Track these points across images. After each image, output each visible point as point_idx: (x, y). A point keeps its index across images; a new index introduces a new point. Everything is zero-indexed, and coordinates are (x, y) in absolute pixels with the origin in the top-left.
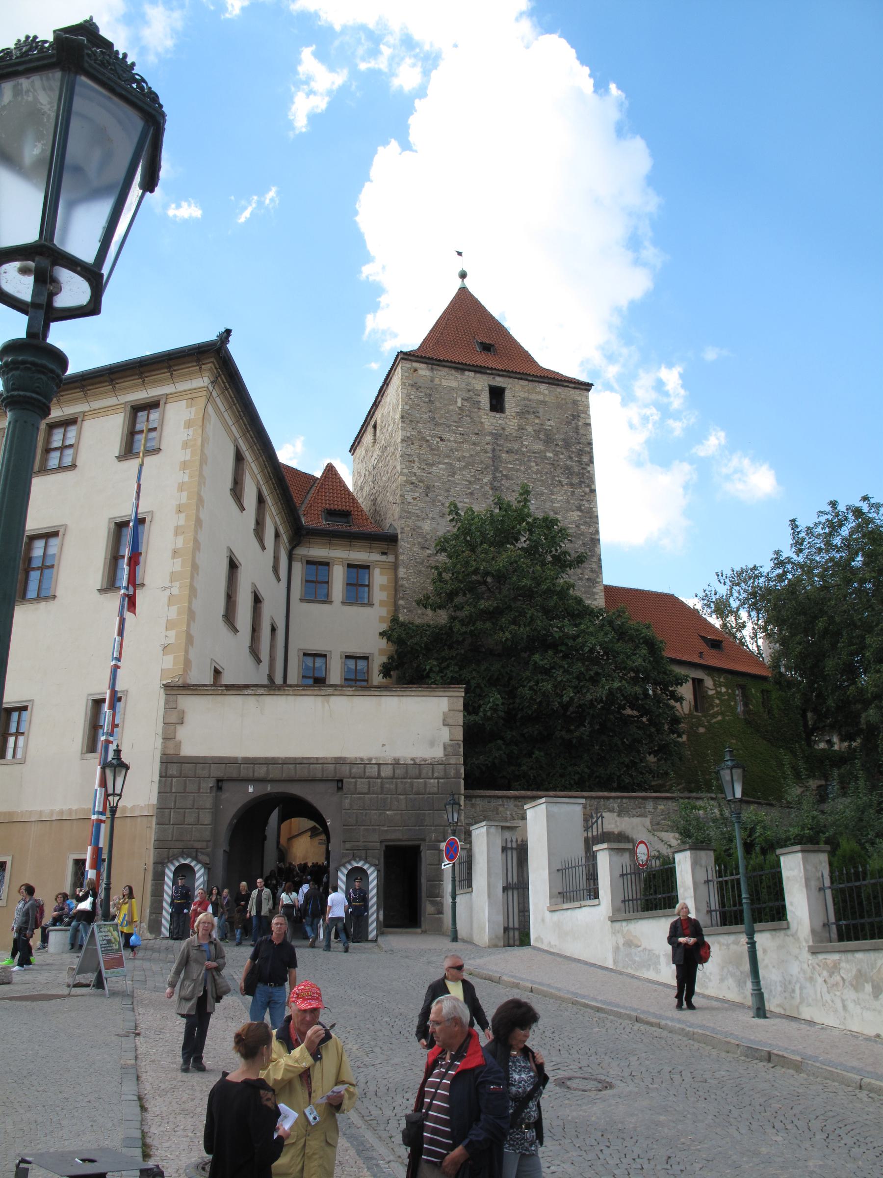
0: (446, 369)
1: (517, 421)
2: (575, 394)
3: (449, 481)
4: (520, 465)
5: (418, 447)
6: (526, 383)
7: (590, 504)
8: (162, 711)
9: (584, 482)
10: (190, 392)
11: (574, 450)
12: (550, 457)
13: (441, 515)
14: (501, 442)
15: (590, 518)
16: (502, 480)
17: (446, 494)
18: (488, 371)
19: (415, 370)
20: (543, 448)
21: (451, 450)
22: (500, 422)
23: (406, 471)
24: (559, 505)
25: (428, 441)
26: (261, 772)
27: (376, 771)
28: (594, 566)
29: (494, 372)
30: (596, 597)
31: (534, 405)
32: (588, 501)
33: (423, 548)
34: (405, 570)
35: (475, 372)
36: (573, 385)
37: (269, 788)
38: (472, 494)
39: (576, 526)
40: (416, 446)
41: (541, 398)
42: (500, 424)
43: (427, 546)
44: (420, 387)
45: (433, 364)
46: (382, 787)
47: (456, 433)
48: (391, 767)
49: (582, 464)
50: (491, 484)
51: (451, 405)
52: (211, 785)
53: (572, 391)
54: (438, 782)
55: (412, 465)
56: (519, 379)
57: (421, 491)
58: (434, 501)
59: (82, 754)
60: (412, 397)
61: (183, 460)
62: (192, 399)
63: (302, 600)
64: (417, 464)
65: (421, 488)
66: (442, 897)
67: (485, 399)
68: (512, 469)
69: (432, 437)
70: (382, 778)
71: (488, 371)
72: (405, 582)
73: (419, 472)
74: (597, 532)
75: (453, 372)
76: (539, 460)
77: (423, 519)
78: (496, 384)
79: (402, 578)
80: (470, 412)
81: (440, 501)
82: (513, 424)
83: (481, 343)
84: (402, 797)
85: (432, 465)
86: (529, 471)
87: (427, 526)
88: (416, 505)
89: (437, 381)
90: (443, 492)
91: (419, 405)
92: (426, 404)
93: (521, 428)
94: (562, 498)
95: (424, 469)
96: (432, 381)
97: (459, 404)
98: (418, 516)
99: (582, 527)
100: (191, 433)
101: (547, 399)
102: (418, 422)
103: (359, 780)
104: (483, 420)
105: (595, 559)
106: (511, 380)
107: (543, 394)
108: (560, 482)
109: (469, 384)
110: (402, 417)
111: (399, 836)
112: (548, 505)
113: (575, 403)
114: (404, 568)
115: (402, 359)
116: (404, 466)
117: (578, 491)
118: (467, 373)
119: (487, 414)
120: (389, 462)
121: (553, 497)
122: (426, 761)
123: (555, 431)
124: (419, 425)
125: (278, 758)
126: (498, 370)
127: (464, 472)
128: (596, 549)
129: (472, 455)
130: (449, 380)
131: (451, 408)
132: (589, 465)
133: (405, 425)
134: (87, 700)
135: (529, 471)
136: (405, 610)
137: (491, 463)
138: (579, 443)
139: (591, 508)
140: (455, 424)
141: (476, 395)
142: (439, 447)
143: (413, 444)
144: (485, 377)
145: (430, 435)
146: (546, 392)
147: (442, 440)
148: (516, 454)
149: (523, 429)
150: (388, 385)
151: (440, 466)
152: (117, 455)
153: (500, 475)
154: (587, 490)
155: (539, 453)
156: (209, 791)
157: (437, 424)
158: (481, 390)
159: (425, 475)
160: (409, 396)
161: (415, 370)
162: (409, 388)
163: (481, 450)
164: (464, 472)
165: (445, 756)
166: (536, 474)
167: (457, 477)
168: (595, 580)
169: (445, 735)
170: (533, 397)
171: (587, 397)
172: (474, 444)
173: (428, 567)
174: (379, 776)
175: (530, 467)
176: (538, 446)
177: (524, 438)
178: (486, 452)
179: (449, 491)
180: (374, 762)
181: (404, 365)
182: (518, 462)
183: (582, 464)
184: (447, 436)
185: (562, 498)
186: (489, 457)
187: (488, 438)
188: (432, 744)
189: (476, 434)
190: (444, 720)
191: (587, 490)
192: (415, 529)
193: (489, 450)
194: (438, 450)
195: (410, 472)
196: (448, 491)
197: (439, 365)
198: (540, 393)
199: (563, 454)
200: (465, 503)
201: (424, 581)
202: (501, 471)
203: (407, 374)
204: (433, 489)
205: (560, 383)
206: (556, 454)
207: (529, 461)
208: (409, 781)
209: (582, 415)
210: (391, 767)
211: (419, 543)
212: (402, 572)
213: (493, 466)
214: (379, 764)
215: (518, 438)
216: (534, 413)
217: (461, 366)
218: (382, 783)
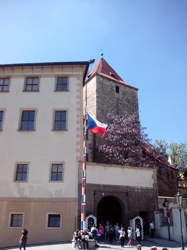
2: (135, 91)
14: (118, 101)
26: (107, 189)
46: (139, 196)
64: (100, 104)
69: (103, 97)
73: (100, 106)
75: (108, 81)
85: (103, 105)
89: (104, 82)
93: (123, 98)
96: (103, 82)
109: (111, 84)
111: (143, 209)
113: (134, 93)
115: (96, 75)
120: (90, 102)
138: (135, 104)
146: (128, 89)
165: (153, 187)
169: (153, 181)
170: (125, 90)
176: (127, 103)
180: (136, 188)
184: (107, 97)
187: (116, 99)
188: (150, 184)
190: (152, 177)
206: (130, 106)
208: (145, 193)
214: (138, 189)
218: (139, 194)
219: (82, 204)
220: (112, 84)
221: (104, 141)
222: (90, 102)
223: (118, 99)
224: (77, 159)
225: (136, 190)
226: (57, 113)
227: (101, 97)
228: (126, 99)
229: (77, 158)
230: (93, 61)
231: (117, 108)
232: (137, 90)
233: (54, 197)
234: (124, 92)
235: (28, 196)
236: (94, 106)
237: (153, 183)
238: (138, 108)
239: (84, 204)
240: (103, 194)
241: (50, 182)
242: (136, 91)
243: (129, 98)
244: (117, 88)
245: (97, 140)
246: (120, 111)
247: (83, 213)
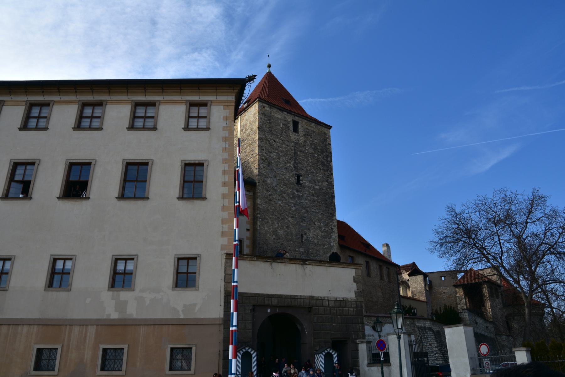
0: (276, 109)
1: (303, 138)
2: (325, 130)
3: (277, 161)
4: (305, 158)
5: (265, 143)
6: (307, 121)
7: (331, 180)
8: (223, 268)
9: (329, 170)
10: (226, 102)
11: (325, 155)
12: (316, 157)
13: (274, 176)
14: (297, 146)
15: (331, 186)
16: (298, 164)
17: (276, 167)
18: (293, 113)
19: (264, 107)
20: (313, 152)
21: (278, 147)
22: (297, 137)
23: (260, 154)
24: (319, 179)
25: (269, 141)
26: (275, 302)
27: (328, 304)
28: (333, 208)
29: (295, 114)
30: (334, 221)
31: (310, 132)
32: (330, 178)
33: (267, 191)
34: (260, 200)
35: (288, 113)
36: (324, 126)
37: (278, 311)
38: (286, 168)
39: (326, 189)
40: (264, 143)
41: (312, 129)
42: (297, 138)
43: (269, 190)
44: (266, 115)
45: (271, 106)
47: (280, 140)
48: (333, 301)
49: (328, 161)
50: (294, 165)
51: (278, 126)
52: (250, 308)
53: (324, 129)
54: (354, 310)
55: (263, 151)
56: (304, 119)
57: (266, 164)
58: (271, 170)
59: (173, 287)
60: (263, 119)
61: (224, 136)
62: (227, 106)
65: (266, 162)
66: (359, 367)
67: (291, 126)
68: (302, 159)
69: (271, 139)
70: (330, 307)
71: (293, 113)
72: (260, 206)
74: (333, 193)
76: (312, 157)
77: (267, 177)
78: (295, 120)
79: (259, 204)
80: (286, 131)
81: (274, 170)
82: (302, 139)
83: (285, 99)
84: (339, 317)
85: (271, 152)
86: (308, 161)
87: (269, 181)
88: (265, 170)
89: (272, 113)
90: (275, 166)
91: (265, 124)
92: (268, 124)
93: (305, 142)
94: (321, 175)
95: (268, 154)
96: (271, 113)
97: (281, 126)
98: (265, 176)
99: (328, 190)
100: (228, 123)
101: (315, 130)
102: (265, 132)
103: (320, 308)
104: (291, 135)
105: (333, 205)
106: (301, 119)
107: (313, 127)
108: (320, 168)
109: (285, 118)
110: (259, 128)
112: (315, 177)
113: (325, 133)
114: (260, 199)
116: (259, 151)
117: (326, 173)
118: (284, 112)
119: (292, 133)
120: (246, 147)
121: (317, 174)
122: (348, 299)
123: (318, 145)
124: (265, 133)
125: (283, 295)
126: (297, 113)
127: (283, 158)
128: (333, 200)
129: (286, 151)
130: (277, 115)
131: (278, 127)
132: (330, 162)
133: (260, 132)
134: (175, 257)
135: (308, 161)
136: (260, 220)
137: (294, 155)
138: (327, 152)
139: (331, 182)
140: (279, 135)
141: (288, 123)
142: (273, 145)
143: (263, 141)
144: (291, 116)
145: (270, 139)
146: (314, 127)
147: (275, 142)
148: (303, 153)
149: (306, 142)
150: (245, 111)
151: (274, 154)
152: (183, 127)
153: (297, 161)
154: (330, 173)
155: (312, 154)
156: (250, 311)
157: (273, 134)
158: (290, 122)
159: (268, 156)
160: (262, 119)
161: (264, 107)
162: (261, 115)
163: (290, 149)
164: (283, 158)
165: (356, 297)
166: (311, 163)
167: (281, 160)
168: (333, 214)
170: (309, 128)
171: (329, 132)
172: (287, 146)
174: (329, 306)
175: (308, 160)
176: (311, 151)
177: (306, 146)
178: (292, 150)
179: (277, 166)
180: (326, 299)
181: (259, 103)
182: (304, 157)
183: (328, 161)
184: (277, 140)
185: (321, 175)
186: (293, 153)
187: (293, 144)
189: (288, 141)
191: (330, 173)
192: (264, 182)
193: (293, 150)
194: (273, 146)
195: (262, 154)
196: (277, 165)
197: (273, 107)
198: (312, 127)
199: (321, 156)
200: (284, 172)
201: (268, 207)
202: (298, 160)
203: (261, 108)
204: (271, 164)
205: (320, 124)
207: (308, 157)
209: (328, 140)
210: (333, 301)
211: (266, 188)
212: (258, 201)
213: (295, 157)
214: (328, 300)
215: (304, 146)
216: (310, 135)
217: (282, 109)
218: (330, 310)
219: (231, 329)
220: (287, 117)
221: (271, 218)
222: (246, 147)
223: (296, 144)
224: (222, 249)
226: (188, 168)
227: (267, 139)
228: (311, 144)
229: (223, 247)
230: (252, 78)
231: (296, 159)
232: (330, 127)
233: (182, 317)
234: (307, 132)
235: (135, 316)
236: (254, 155)
237: (356, 290)
238: (331, 159)
239: (234, 328)
240: (269, 311)
241: (173, 290)
242: (329, 130)
243: (316, 142)
244: (295, 124)
245: (259, 215)
246: (300, 163)
247: (232, 344)
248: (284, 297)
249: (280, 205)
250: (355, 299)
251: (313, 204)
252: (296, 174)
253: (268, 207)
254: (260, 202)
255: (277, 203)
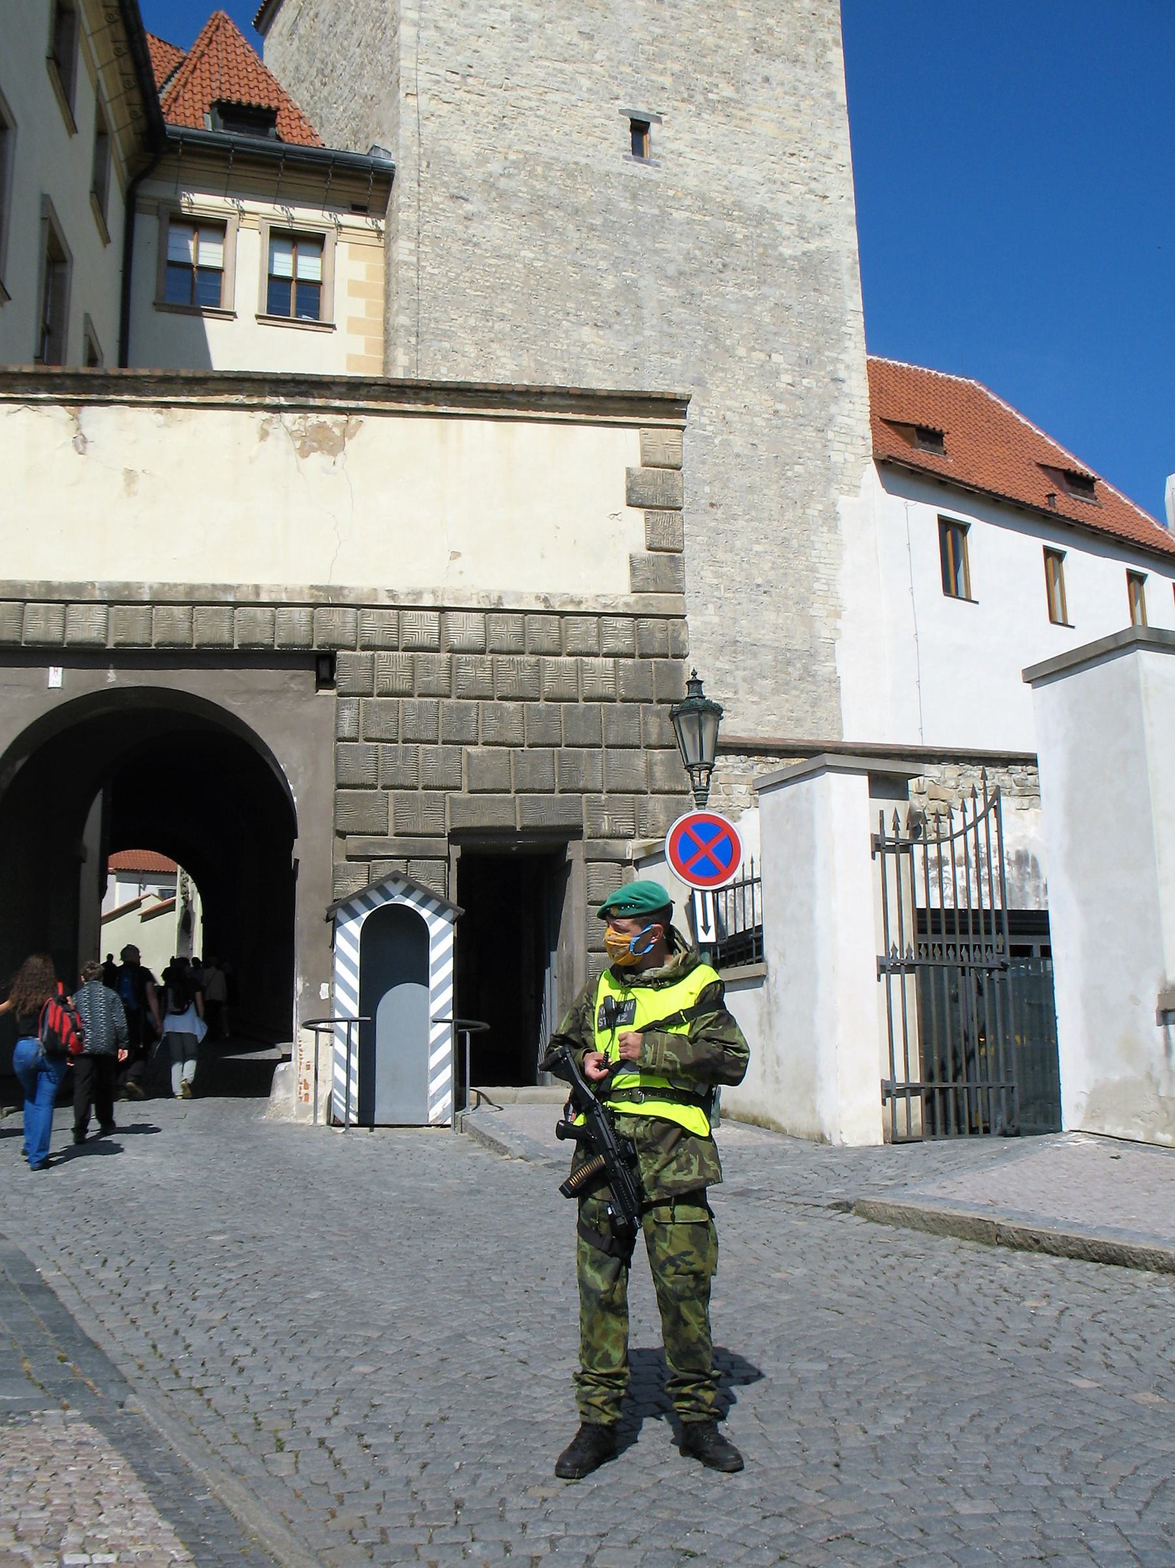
34: (412, 246)
63: (160, 305)
79: (406, 263)
122: (580, 603)
125: (140, 586)
173: (467, 242)
190: (630, 490)
211: (445, 184)
225: (424, 628)
248: (146, 598)
249: (529, 267)
250: (627, 604)
251: (728, 260)
252: (622, 112)
253: (458, 275)
254: (411, 252)
255: (509, 257)
